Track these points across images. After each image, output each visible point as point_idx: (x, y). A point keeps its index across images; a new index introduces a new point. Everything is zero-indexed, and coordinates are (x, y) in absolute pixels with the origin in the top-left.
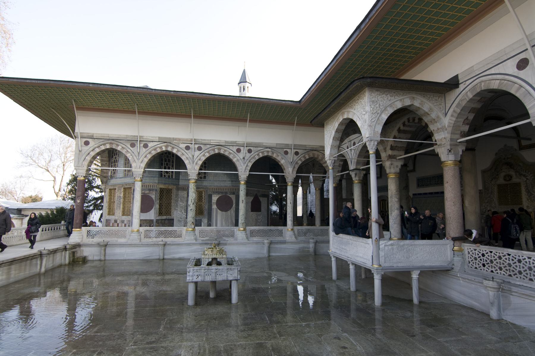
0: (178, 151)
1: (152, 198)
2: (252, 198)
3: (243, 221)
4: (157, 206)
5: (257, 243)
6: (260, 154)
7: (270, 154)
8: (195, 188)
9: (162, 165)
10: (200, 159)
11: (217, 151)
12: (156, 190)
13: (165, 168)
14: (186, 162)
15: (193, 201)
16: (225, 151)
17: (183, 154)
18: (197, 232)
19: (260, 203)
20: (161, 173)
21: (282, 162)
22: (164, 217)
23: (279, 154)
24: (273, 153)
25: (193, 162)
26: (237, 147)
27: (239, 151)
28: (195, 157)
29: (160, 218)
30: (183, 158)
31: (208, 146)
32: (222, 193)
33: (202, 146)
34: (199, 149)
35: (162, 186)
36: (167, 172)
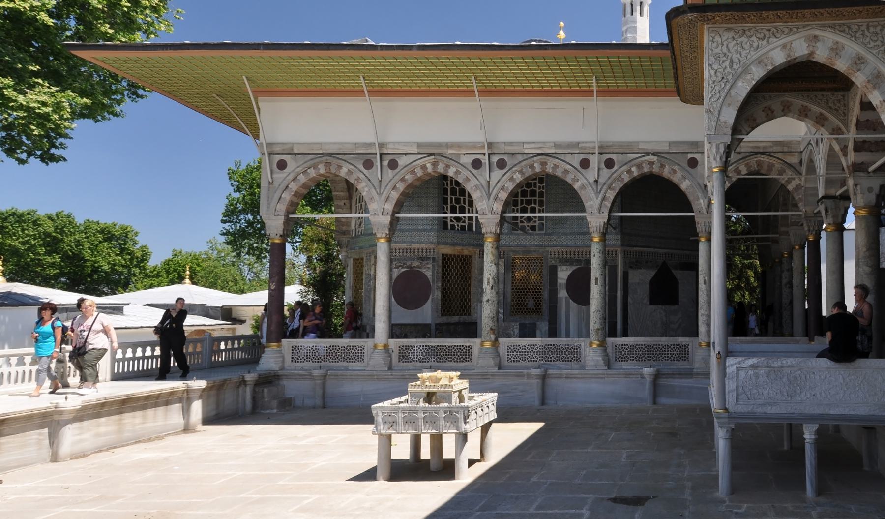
0: (457, 172)
1: (426, 277)
2: (648, 274)
3: (598, 326)
4: (437, 294)
5: (627, 375)
6: (634, 169)
7: (656, 169)
8: (495, 251)
9: (446, 203)
10: (503, 189)
11: (538, 169)
12: (434, 259)
13: (453, 211)
14: (475, 196)
15: (491, 282)
16: (556, 167)
17: (467, 179)
18: (502, 350)
19: (675, 283)
20: (444, 223)
21: (685, 186)
22: (455, 319)
23: (676, 168)
24: (662, 166)
25: (489, 195)
26: (582, 157)
27: (585, 164)
28: (493, 183)
29: (445, 319)
30: (469, 187)
31: (520, 158)
32: (578, 262)
33: (506, 157)
34: (501, 164)
35: (447, 250)
36: (458, 219)
